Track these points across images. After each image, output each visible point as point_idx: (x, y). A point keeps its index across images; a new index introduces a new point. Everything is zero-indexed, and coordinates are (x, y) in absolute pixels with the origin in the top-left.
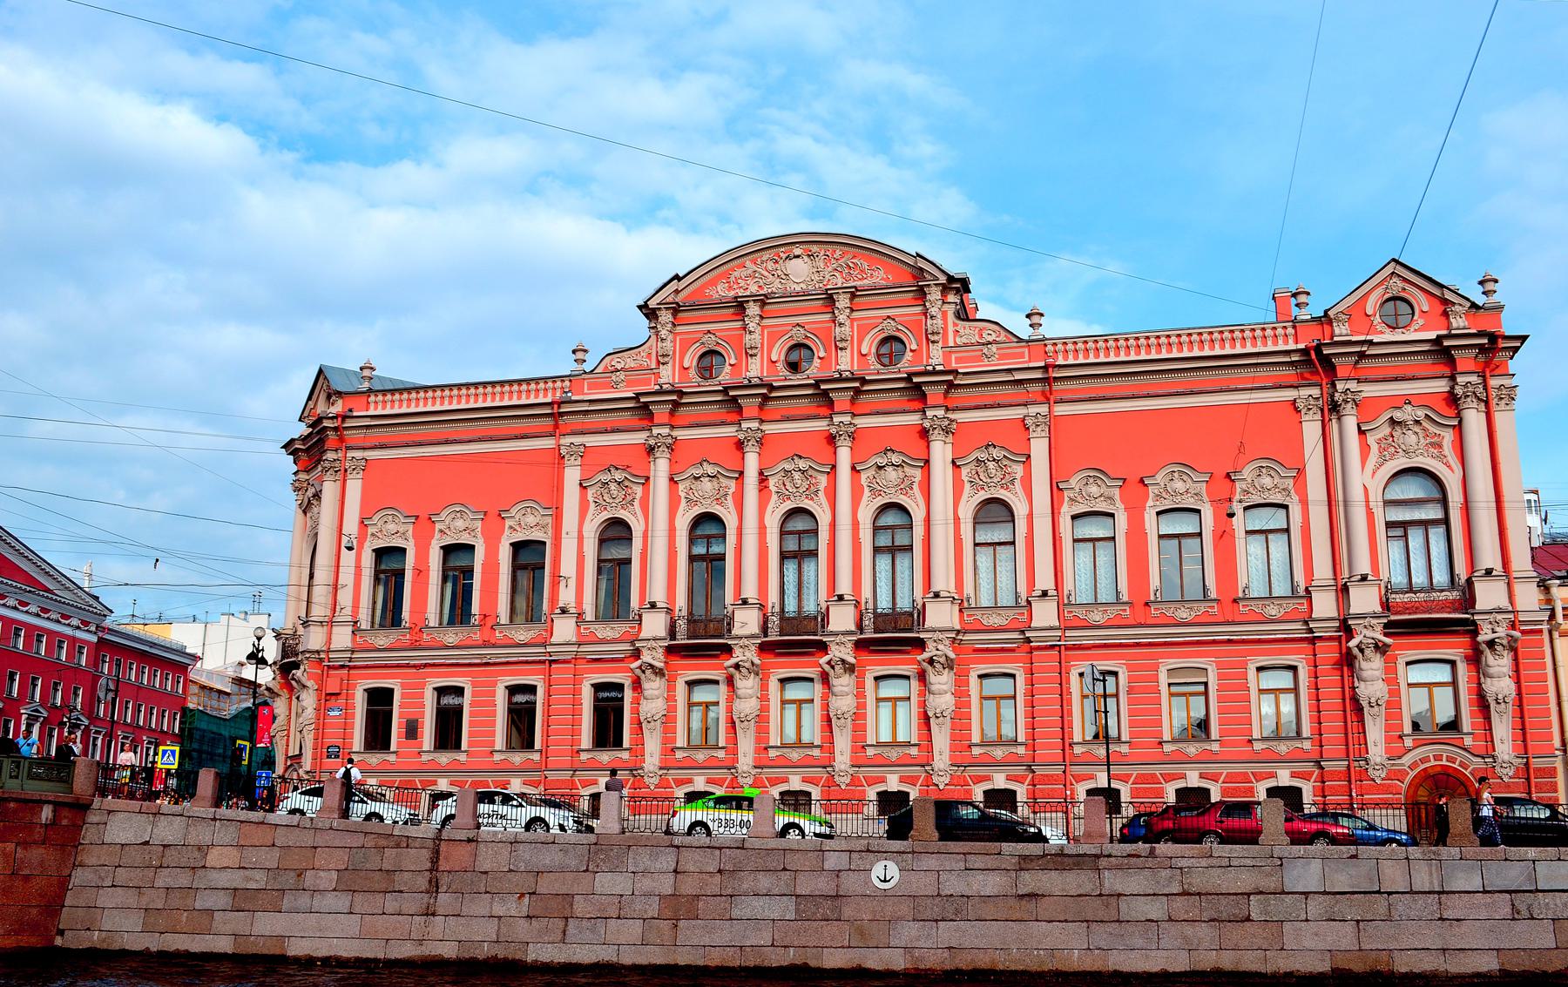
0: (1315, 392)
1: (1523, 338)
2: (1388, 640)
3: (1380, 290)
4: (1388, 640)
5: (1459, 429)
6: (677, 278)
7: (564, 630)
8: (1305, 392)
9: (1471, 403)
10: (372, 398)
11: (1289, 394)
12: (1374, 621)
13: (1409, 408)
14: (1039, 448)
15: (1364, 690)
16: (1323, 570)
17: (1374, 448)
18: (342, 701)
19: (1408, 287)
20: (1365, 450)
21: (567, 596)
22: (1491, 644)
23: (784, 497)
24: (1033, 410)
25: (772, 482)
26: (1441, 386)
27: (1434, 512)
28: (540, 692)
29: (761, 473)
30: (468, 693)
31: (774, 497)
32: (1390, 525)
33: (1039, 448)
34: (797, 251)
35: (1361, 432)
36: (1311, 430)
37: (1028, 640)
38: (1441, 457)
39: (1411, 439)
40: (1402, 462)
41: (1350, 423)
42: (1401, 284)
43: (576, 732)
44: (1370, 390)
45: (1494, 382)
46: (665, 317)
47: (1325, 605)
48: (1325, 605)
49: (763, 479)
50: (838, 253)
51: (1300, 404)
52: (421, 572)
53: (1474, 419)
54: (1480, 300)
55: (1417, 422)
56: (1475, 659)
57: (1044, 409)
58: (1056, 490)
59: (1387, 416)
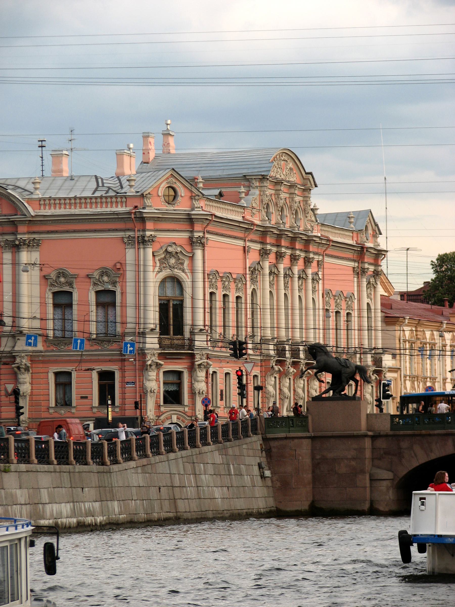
3: (165, 183)
5: (192, 258)
12: (155, 352)
13: (174, 246)
17: (158, 264)
19: (177, 182)
26: (186, 235)
35: (154, 256)
38: (183, 271)
39: (172, 261)
41: (150, 251)
42: (174, 180)
44: (160, 235)
53: (199, 253)
55: (177, 253)
56: (192, 369)
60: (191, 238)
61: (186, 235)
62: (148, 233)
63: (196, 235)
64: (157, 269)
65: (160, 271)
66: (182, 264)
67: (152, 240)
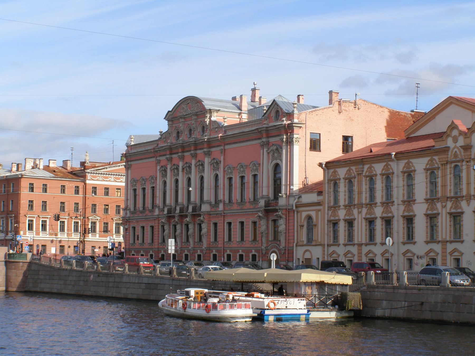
6: (169, 112)
18: (128, 231)
29: (182, 167)
64: (270, 161)
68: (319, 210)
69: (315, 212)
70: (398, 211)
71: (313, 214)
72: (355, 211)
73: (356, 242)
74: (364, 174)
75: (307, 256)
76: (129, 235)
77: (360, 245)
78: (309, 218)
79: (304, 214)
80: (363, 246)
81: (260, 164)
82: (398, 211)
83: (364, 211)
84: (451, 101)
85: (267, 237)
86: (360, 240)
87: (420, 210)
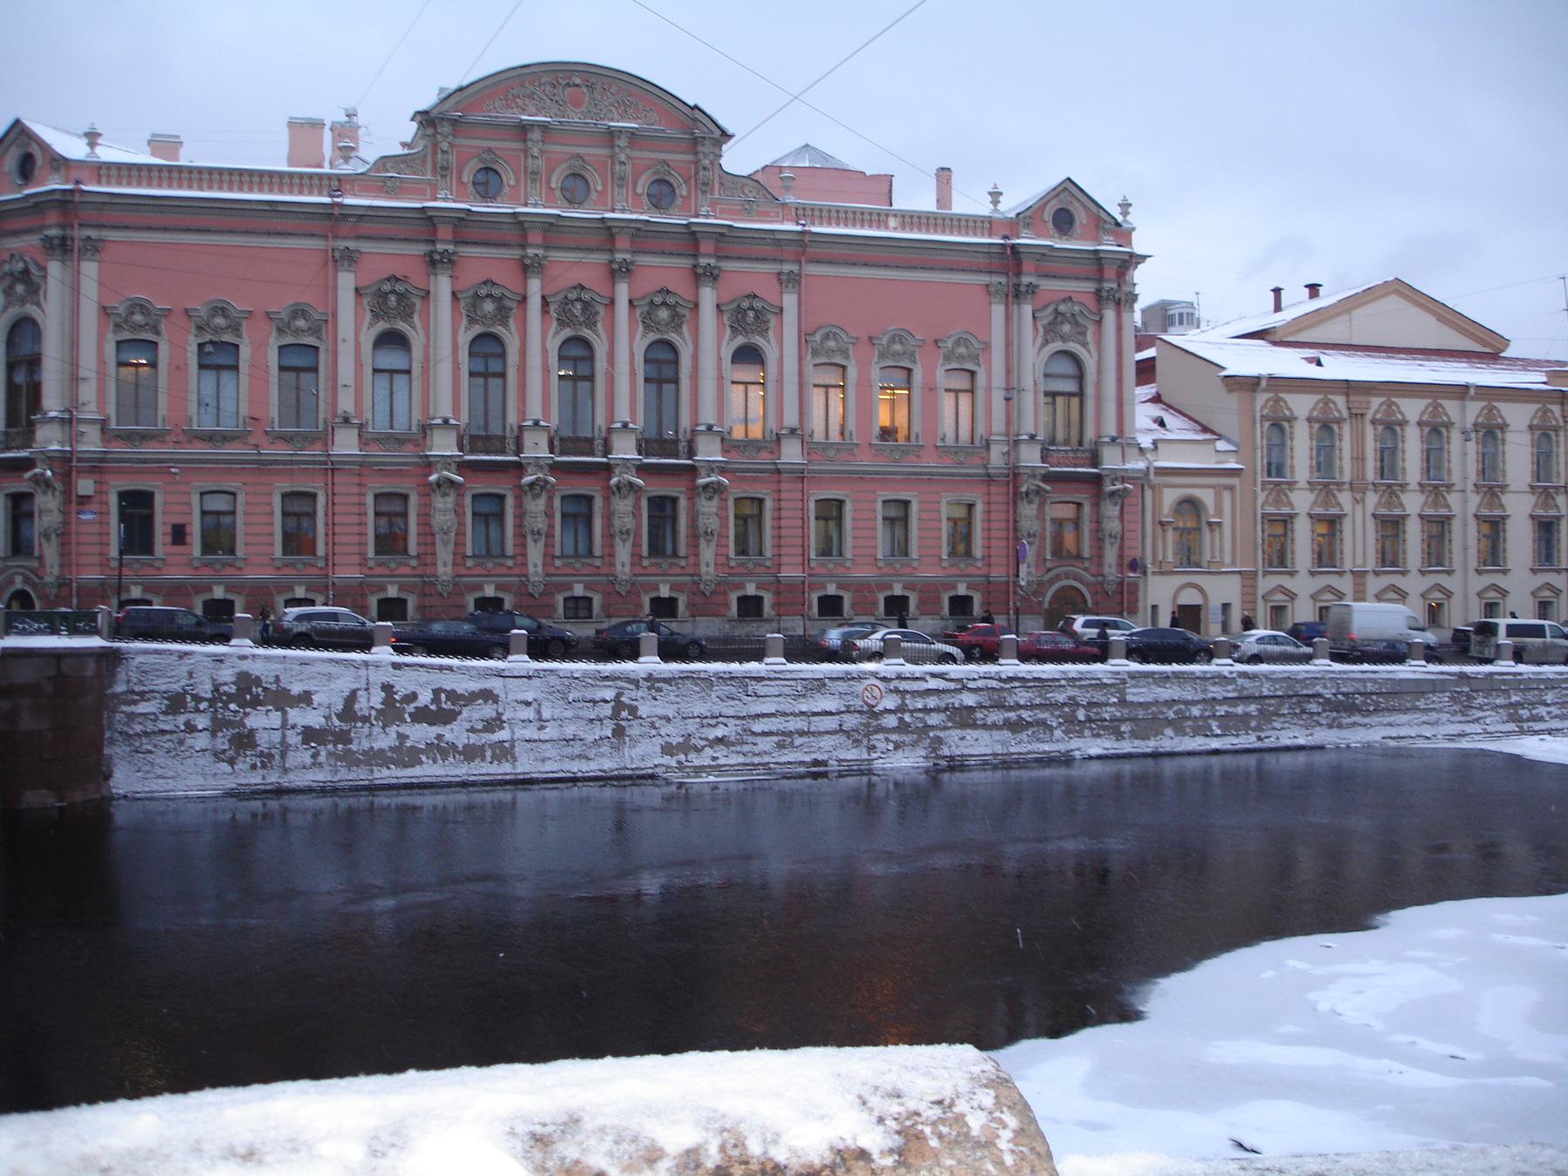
0: (1003, 280)
1: (1143, 258)
2: (1048, 488)
3: (1054, 202)
4: (1048, 488)
5: (1099, 323)
7: (346, 444)
8: (996, 279)
9: (1112, 305)
10: (104, 172)
11: (984, 279)
14: (790, 301)
15: (1025, 525)
16: (998, 425)
17: (1041, 331)
18: (95, 507)
20: (1036, 328)
21: (346, 403)
22: (1112, 494)
23: (562, 323)
24: (786, 268)
25: (552, 308)
26: (1090, 287)
27: (1070, 386)
28: (321, 500)
30: (241, 498)
31: (555, 324)
32: (1047, 394)
33: (790, 301)
34: (578, 81)
35: (1034, 318)
36: (998, 310)
37: (779, 471)
38: (1085, 345)
39: (1066, 328)
40: (1058, 345)
41: (1027, 309)
43: (363, 544)
44: (1047, 285)
45: (1125, 289)
46: (446, 128)
47: (996, 457)
48: (996, 457)
49: (545, 303)
50: (614, 89)
51: (992, 289)
52: (178, 369)
53: (1109, 315)
54: (1120, 219)
57: (795, 268)
58: (804, 337)
59: (1051, 309)
60: (1098, 293)
61: (1090, 287)
62: (1025, 280)
63: (1106, 285)
64: (1039, 340)
65: (1046, 342)
66: (1084, 334)
67: (1032, 289)
68: (1231, 488)
69: (1211, 491)
70: (1464, 505)
71: (1206, 497)
72: (1345, 498)
73: (1348, 566)
74: (1369, 417)
75: (1190, 598)
76: (104, 523)
77: (1359, 575)
78: (1191, 505)
79: (1170, 497)
80: (1370, 578)
81: (987, 346)
82: (1464, 505)
83: (1372, 499)
84: (1400, 289)
85: (459, 544)
86: (1359, 561)
87: (1519, 508)
